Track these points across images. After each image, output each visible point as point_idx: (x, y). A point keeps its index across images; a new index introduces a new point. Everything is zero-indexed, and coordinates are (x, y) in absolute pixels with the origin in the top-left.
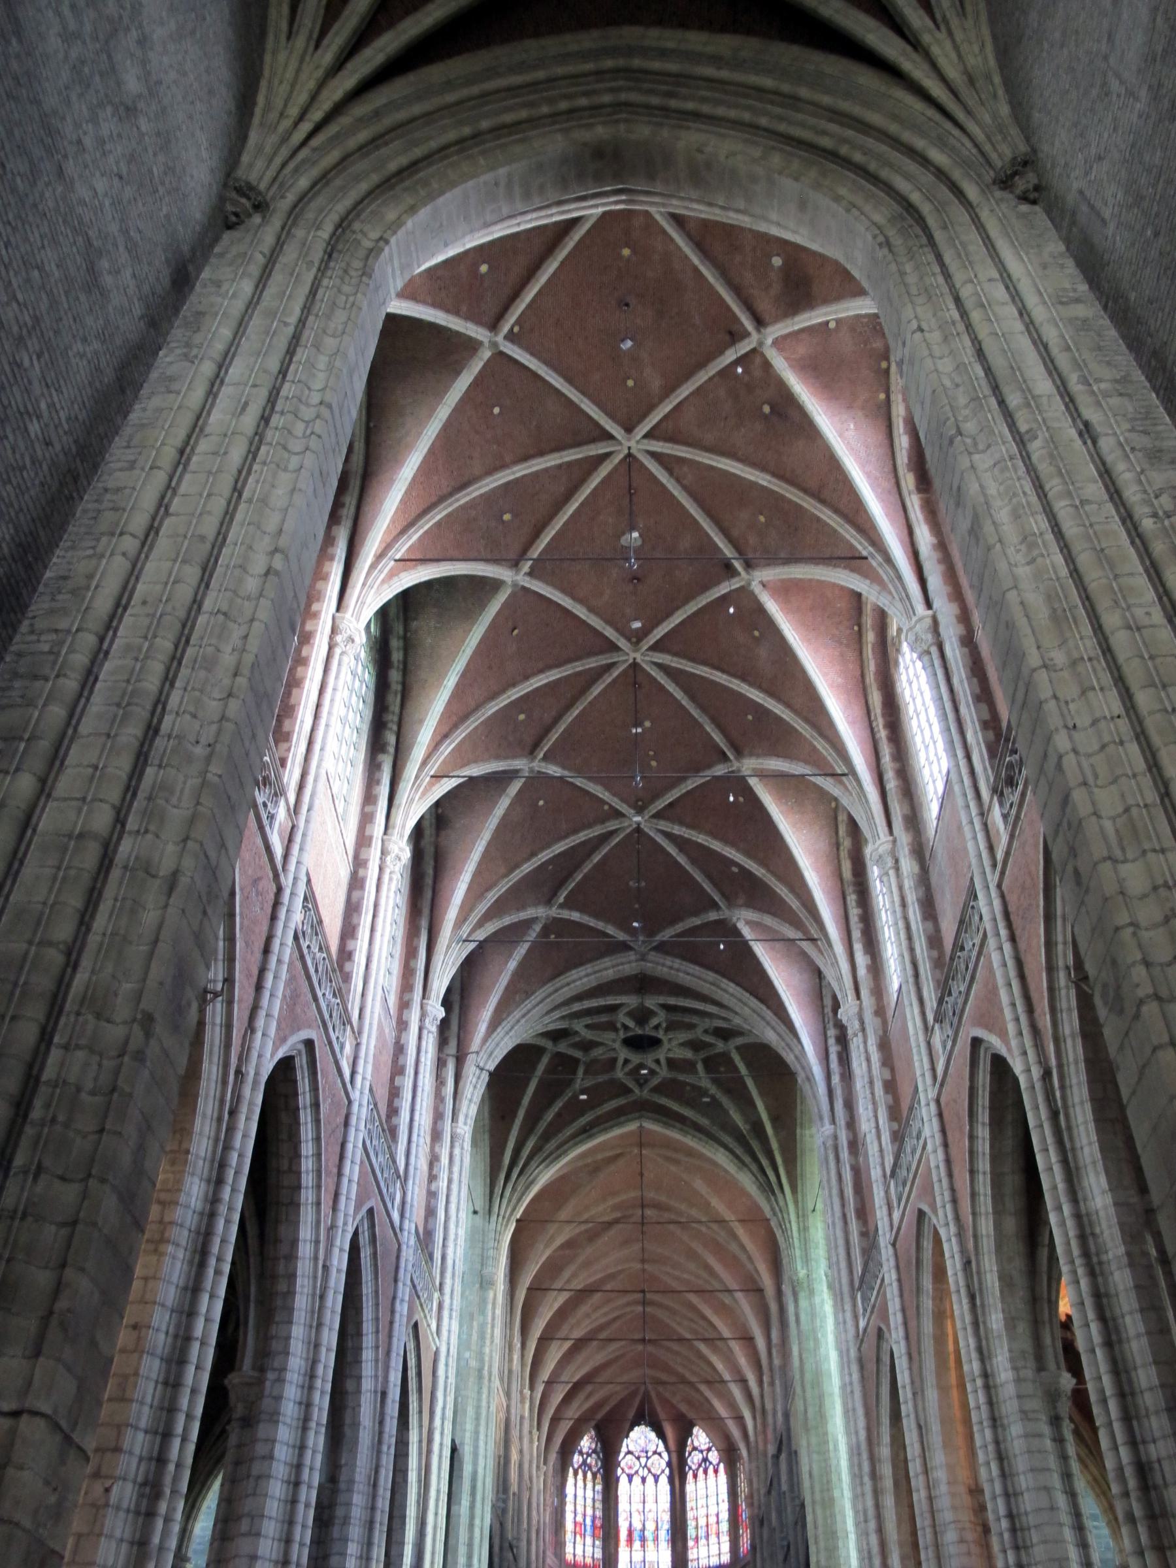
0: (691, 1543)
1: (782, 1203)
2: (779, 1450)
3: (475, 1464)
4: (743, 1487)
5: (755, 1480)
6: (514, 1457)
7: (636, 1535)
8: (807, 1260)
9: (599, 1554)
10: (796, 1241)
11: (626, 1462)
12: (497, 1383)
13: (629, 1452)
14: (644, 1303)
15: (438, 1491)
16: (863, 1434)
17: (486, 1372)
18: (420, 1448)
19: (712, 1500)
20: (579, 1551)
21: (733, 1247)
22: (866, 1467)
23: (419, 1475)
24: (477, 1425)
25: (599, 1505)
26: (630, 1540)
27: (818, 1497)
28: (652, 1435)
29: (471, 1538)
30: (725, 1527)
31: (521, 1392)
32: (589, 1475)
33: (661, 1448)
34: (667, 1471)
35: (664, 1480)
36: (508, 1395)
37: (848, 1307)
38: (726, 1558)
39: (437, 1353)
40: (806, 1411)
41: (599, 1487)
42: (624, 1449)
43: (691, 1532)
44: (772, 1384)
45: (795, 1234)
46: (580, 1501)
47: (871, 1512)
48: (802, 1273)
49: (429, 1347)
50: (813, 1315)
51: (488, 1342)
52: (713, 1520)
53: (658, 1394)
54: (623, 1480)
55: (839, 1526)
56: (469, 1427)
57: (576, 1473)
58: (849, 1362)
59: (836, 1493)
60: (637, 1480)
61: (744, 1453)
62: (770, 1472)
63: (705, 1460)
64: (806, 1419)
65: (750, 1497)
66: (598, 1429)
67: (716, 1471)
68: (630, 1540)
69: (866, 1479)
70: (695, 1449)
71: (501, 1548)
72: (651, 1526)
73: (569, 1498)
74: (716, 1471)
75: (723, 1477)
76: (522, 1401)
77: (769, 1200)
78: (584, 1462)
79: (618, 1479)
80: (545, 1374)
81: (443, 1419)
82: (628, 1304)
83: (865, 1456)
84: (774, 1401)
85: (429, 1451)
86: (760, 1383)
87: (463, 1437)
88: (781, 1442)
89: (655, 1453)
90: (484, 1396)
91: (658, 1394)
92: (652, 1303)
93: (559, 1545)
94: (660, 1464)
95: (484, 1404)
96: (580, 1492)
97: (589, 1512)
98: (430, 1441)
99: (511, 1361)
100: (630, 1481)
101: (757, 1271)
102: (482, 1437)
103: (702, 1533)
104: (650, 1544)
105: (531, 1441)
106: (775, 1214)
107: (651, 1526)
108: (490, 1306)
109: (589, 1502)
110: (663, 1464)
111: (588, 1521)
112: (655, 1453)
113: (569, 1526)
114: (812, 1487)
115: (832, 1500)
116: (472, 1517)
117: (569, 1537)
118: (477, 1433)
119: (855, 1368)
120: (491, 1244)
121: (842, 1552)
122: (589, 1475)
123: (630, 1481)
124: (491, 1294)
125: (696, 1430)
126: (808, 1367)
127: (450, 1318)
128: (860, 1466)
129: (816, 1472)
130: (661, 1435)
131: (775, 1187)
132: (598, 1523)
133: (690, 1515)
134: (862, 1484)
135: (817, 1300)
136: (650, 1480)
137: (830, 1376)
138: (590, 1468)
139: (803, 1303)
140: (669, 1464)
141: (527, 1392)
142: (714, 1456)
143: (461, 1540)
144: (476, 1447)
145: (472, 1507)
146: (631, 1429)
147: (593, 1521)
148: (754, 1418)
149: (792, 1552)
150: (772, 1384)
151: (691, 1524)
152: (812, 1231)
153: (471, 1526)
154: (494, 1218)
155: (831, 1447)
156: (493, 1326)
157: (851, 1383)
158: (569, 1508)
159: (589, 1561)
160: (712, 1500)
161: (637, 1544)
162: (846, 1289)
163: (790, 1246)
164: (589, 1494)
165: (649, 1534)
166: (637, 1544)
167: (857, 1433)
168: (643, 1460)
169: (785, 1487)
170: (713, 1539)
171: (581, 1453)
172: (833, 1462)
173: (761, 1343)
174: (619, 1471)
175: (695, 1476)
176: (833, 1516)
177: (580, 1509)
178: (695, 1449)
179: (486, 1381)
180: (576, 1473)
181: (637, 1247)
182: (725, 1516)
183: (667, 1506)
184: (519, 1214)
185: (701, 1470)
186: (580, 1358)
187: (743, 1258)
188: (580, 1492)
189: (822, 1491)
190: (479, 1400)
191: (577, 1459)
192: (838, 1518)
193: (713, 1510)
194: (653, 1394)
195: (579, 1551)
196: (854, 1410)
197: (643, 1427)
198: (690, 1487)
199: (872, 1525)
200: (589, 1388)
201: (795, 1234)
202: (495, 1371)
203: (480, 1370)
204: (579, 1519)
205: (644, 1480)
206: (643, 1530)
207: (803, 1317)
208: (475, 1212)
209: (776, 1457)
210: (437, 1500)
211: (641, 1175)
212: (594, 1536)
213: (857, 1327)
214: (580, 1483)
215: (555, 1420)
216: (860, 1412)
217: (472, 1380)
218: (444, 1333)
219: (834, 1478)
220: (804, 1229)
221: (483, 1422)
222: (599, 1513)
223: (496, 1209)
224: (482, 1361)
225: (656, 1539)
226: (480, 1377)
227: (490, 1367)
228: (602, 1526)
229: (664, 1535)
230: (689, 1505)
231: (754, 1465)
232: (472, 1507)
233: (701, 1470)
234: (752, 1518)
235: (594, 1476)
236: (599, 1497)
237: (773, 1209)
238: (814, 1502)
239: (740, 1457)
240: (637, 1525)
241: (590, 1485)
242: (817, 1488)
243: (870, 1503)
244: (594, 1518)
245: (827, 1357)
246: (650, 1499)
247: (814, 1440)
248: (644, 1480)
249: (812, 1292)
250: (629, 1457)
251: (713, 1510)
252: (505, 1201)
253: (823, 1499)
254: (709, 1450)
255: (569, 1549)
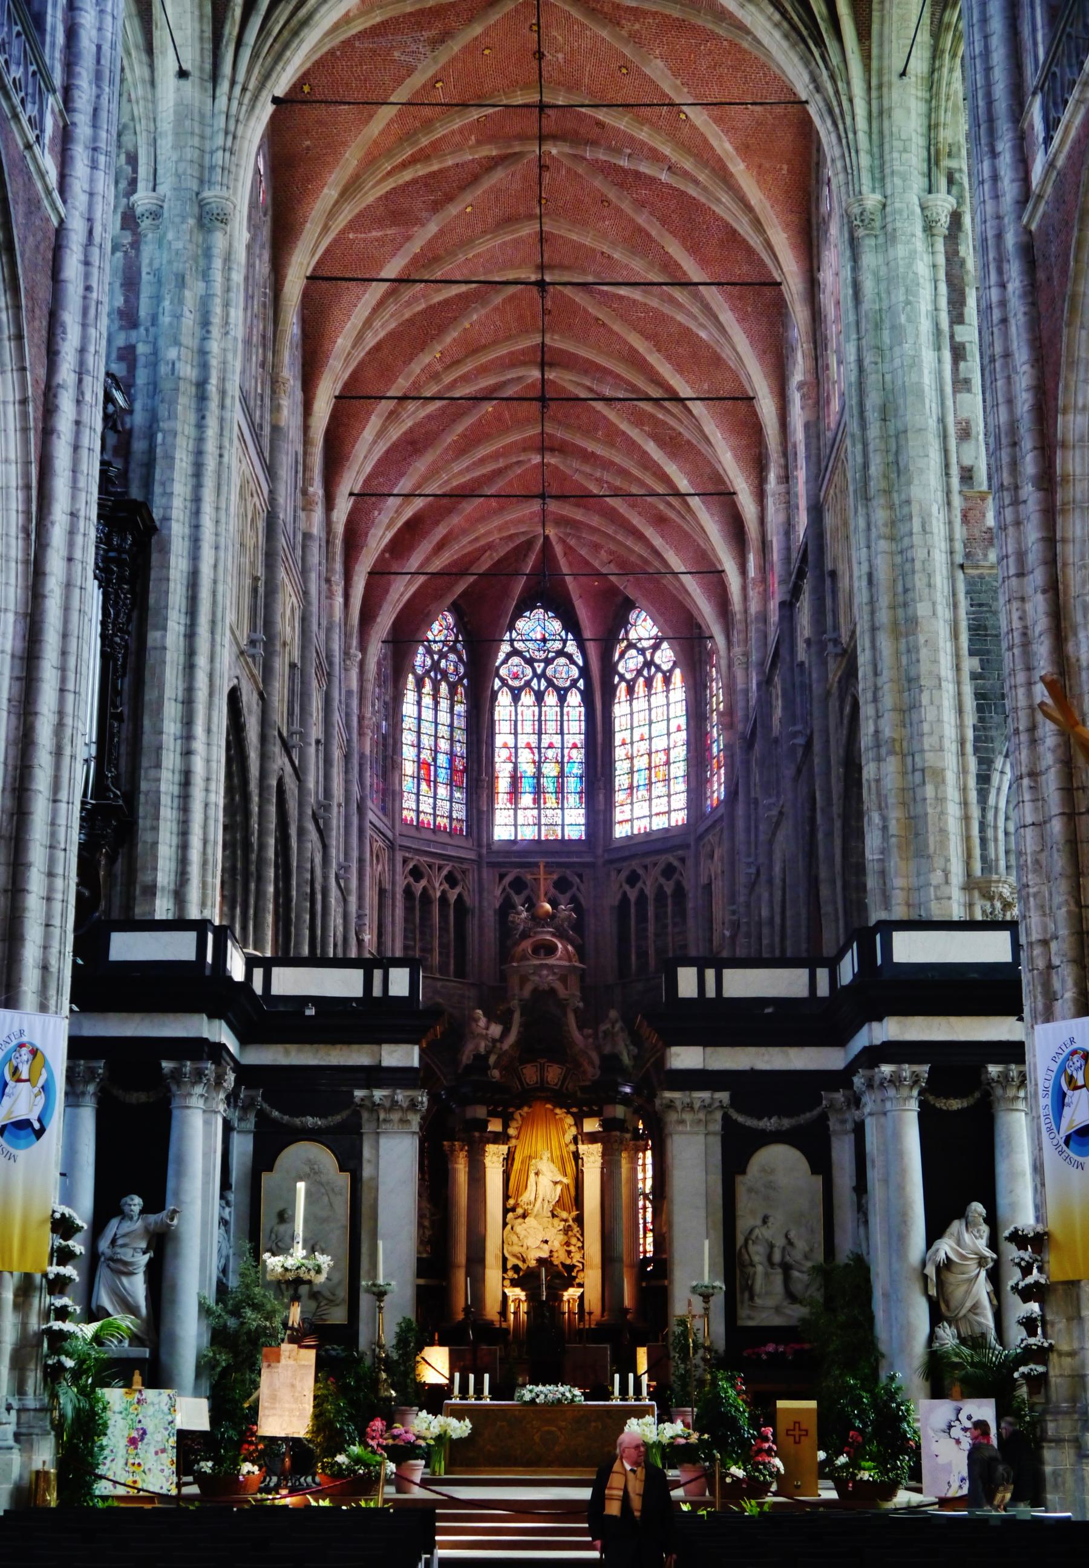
0: (620, 797)
1: (835, 60)
2: (796, 592)
3: (195, 557)
4: (717, 698)
5: (739, 674)
6: (288, 601)
7: (526, 785)
8: (881, 176)
9: (460, 812)
10: (862, 138)
11: (509, 668)
12: (237, 415)
13: (515, 652)
14: (545, 358)
15: (73, 515)
16: (1024, 401)
17: (212, 388)
18: (24, 415)
19: (659, 728)
20: (426, 806)
21: (725, 208)
22: (1029, 466)
23: (27, 475)
24: (198, 487)
25: (460, 735)
26: (514, 793)
27: (884, 616)
28: (556, 626)
29: (190, 690)
30: (679, 769)
31: (305, 492)
32: (444, 688)
33: (571, 647)
34: (581, 684)
35: (574, 698)
36: (271, 471)
37: (1005, 146)
38: (679, 818)
39: (61, 231)
40: (866, 466)
41: (460, 708)
42: (505, 648)
43: (621, 780)
44: (786, 478)
45: (861, 124)
46: (427, 728)
47: (1034, 555)
48: (872, 200)
49: (33, 205)
50: (889, 280)
51: (216, 331)
52: (659, 758)
53: (569, 550)
54: (504, 698)
55: (924, 668)
56: (182, 486)
57: (420, 684)
58: (1000, 261)
59: (922, 609)
60: (527, 699)
61: (720, 640)
62: (772, 638)
63: (648, 664)
64: (866, 479)
65: (730, 711)
66: (455, 609)
67: (667, 681)
68: (514, 793)
69: (1029, 492)
70: (631, 645)
71: (263, 738)
72: (550, 770)
73: (409, 723)
74: (667, 681)
75: (678, 692)
76: (307, 507)
77: (807, 60)
78: (435, 665)
79: (494, 695)
80: (351, 481)
81: (81, 372)
82: (514, 361)
83: (1027, 443)
84: (789, 506)
85: (47, 433)
86: (760, 495)
87: (168, 507)
88: (801, 574)
89: (561, 653)
90: (211, 432)
91: (569, 550)
92: (562, 449)
93: (390, 796)
94: (565, 671)
95: (210, 447)
96: (427, 714)
97: (444, 745)
98: (49, 410)
99: (276, 409)
100: (516, 698)
101: (769, 245)
102: (207, 508)
103: (640, 778)
104: (551, 800)
105: (330, 596)
106: (818, 89)
107: (550, 770)
108: (218, 263)
109: (444, 731)
110: (575, 672)
111: (442, 760)
112: (561, 653)
113: (409, 768)
114: (872, 602)
115: (913, 622)
116: (191, 653)
117: (408, 784)
118: (197, 500)
119: (1014, 270)
120: (219, 140)
121: (929, 714)
122: (444, 688)
123: (516, 698)
124: (219, 241)
125: (633, 616)
126: (872, 379)
127: (94, 167)
128: (1014, 465)
129: (883, 574)
130: (571, 624)
131: (823, 26)
132: (459, 765)
133: (620, 753)
134: (1016, 502)
135: (901, 251)
136: (551, 699)
137: (920, 395)
138: (445, 674)
139: (869, 259)
140: (585, 672)
141: (317, 489)
142: (665, 656)
143: (169, 693)
144: (196, 527)
145: (191, 635)
146: (518, 614)
147: (451, 761)
148: (743, 571)
149: (817, 747)
150: (786, 478)
151: (621, 767)
152: (898, 114)
153: (190, 668)
154: (224, 86)
155: (916, 526)
156: (226, 305)
157: (1003, 303)
158: (408, 737)
159: (443, 822)
160: (659, 728)
161: (527, 800)
162: (1002, 106)
163: (849, 148)
164: (444, 717)
165: (549, 785)
166: (527, 800)
167: (1010, 402)
168: (539, 667)
169: (802, 655)
170: (659, 789)
171: (429, 651)
172: (920, 554)
173: (767, 408)
174: (497, 683)
175: (630, 690)
176: (912, 650)
177: (427, 741)
178: (631, 645)
179: (213, 405)
180: (420, 684)
181: (528, 230)
182: (680, 753)
183: (580, 739)
184: (281, 85)
185: (641, 680)
186: (421, 465)
187: (744, 228)
188: (427, 714)
189: (893, 607)
190: (200, 440)
191: (421, 660)
192: (924, 653)
193: (660, 744)
194: (558, 549)
195: (426, 806)
196: (1007, 355)
197: (539, 613)
198: (620, 709)
199: (1037, 577)
200: (440, 531)
201: (861, 124)
202: (233, 389)
203: (201, 385)
204: (426, 755)
205: (539, 697)
206: (538, 775)
207: (868, 286)
208: (182, 74)
209: (788, 607)
210: (72, 532)
211: (540, 55)
212: (451, 784)
213: (1026, 180)
214: (427, 701)
215: (379, 577)
216: (1022, 355)
217: (185, 403)
218: (79, 198)
219: (919, 581)
220: (879, 114)
221: (209, 482)
222: (460, 749)
223: (227, 68)
224: (204, 367)
225: (560, 791)
226: (202, 397)
227: (223, 380)
228: (466, 769)
229: (573, 784)
230: (618, 739)
231: (737, 650)
232: (191, 635)
233: (641, 680)
234: (728, 747)
235: (453, 689)
236: (460, 723)
237: (814, 79)
238: (874, 629)
239: (714, 651)
240: (527, 769)
241: (444, 704)
242: (884, 601)
243: (1033, 534)
244: (452, 755)
245: (915, 362)
246: (551, 727)
247: (880, 515)
248: (539, 697)
249: (890, 237)
250: (516, 660)
251: (660, 744)
252: (246, 54)
253: (895, 623)
254: (656, 647)
255: (409, 802)
